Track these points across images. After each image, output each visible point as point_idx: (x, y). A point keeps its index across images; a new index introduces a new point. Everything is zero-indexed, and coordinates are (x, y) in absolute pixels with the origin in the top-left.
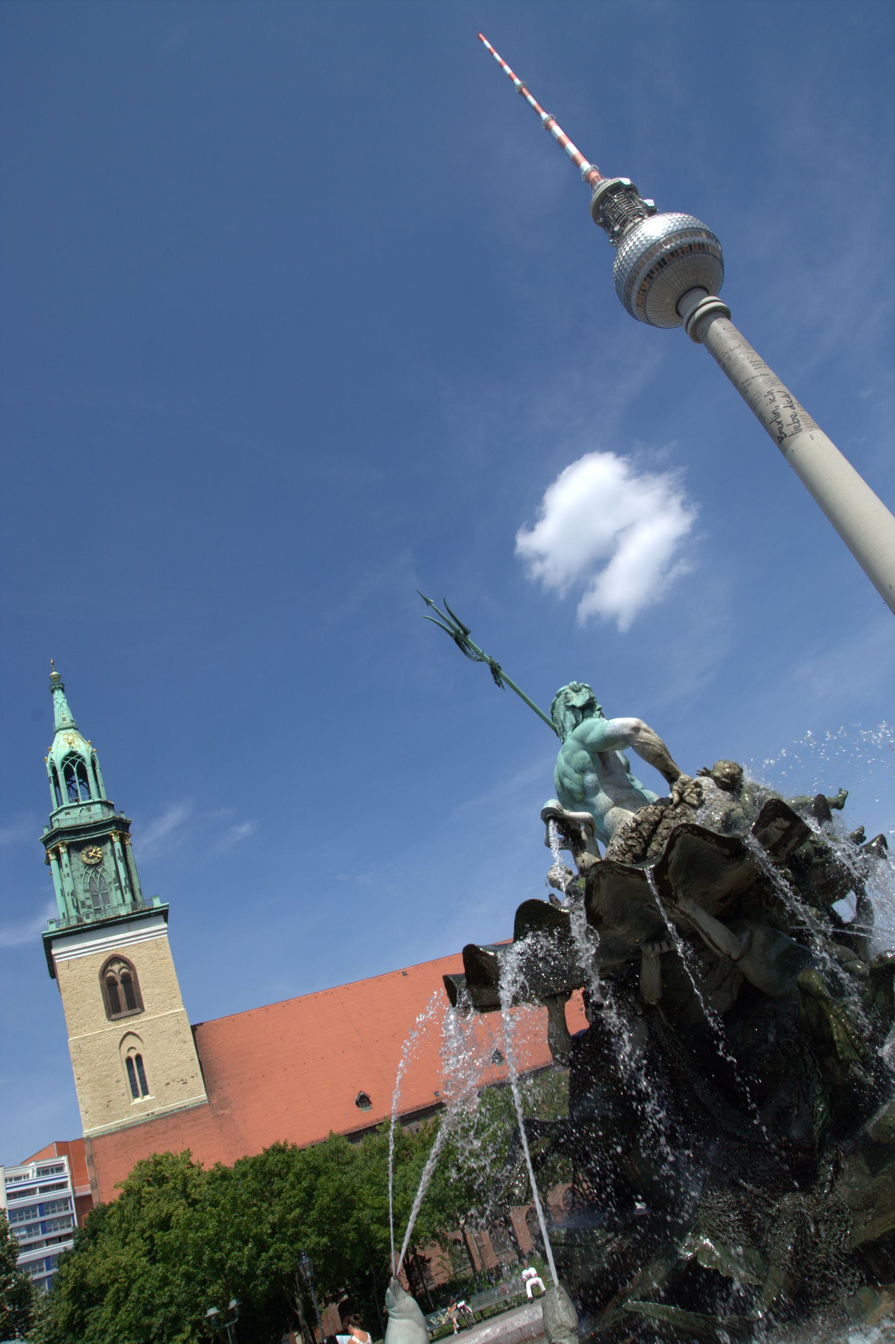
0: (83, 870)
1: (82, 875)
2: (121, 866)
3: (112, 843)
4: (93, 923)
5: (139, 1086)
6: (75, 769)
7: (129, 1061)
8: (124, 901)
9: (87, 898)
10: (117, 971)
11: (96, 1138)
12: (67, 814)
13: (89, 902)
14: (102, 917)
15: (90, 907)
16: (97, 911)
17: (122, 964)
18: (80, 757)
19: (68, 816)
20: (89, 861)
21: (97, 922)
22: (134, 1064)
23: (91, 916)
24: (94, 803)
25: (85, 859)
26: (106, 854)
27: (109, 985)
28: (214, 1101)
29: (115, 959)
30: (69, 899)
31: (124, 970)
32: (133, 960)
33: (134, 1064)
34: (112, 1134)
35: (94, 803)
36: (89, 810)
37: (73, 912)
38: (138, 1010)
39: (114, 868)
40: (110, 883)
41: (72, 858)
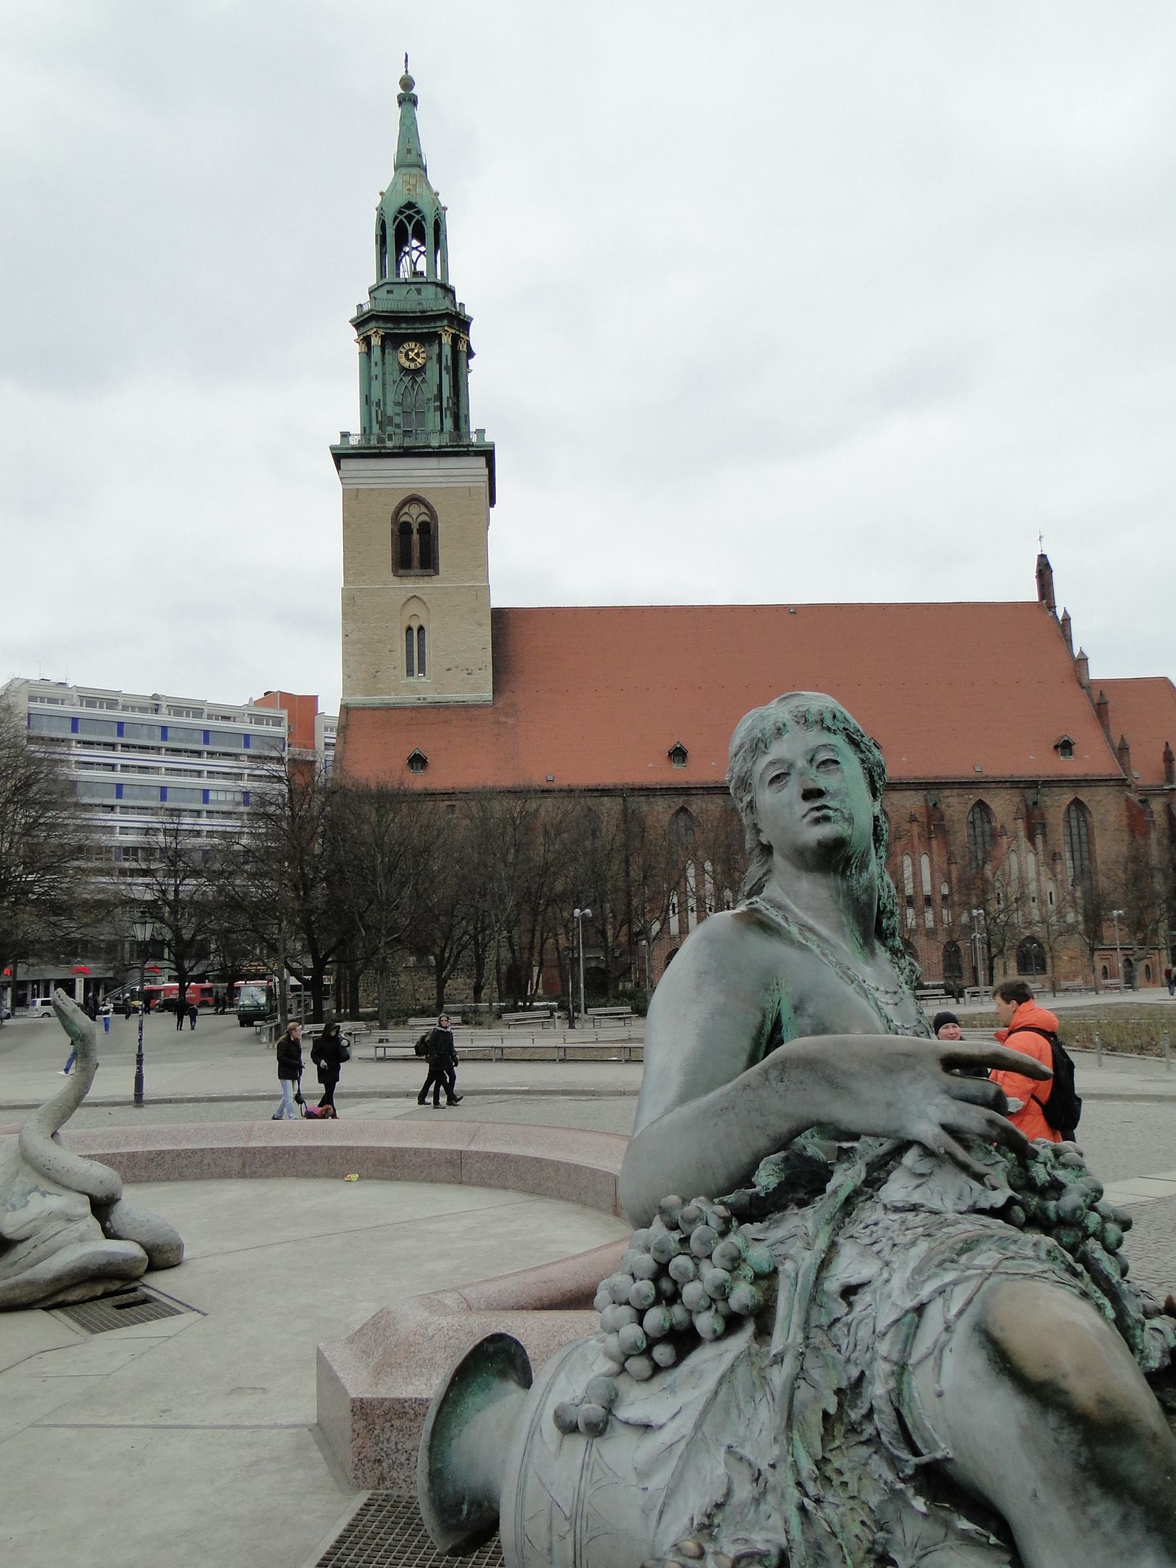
0: (397, 375)
1: (394, 382)
2: (446, 379)
4: (395, 447)
5: (416, 661)
6: (410, 229)
7: (409, 629)
8: (442, 429)
11: (356, 709)
12: (389, 292)
13: (397, 420)
14: (408, 442)
15: (398, 426)
16: (407, 433)
17: (424, 509)
18: (418, 212)
19: (390, 296)
20: (407, 364)
21: (400, 447)
22: (415, 636)
24: (427, 283)
25: (403, 360)
26: (431, 358)
27: (402, 531)
28: (498, 705)
29: (414, 500)
30: (374, 408)
31: (424, 518)
32: (437, 508)
33: (415, 636)
34: (374, 709)
35: (427, 283)
36: (419, 292)
37: (376, 428)
38: (431, 571)
41: (386, 356)
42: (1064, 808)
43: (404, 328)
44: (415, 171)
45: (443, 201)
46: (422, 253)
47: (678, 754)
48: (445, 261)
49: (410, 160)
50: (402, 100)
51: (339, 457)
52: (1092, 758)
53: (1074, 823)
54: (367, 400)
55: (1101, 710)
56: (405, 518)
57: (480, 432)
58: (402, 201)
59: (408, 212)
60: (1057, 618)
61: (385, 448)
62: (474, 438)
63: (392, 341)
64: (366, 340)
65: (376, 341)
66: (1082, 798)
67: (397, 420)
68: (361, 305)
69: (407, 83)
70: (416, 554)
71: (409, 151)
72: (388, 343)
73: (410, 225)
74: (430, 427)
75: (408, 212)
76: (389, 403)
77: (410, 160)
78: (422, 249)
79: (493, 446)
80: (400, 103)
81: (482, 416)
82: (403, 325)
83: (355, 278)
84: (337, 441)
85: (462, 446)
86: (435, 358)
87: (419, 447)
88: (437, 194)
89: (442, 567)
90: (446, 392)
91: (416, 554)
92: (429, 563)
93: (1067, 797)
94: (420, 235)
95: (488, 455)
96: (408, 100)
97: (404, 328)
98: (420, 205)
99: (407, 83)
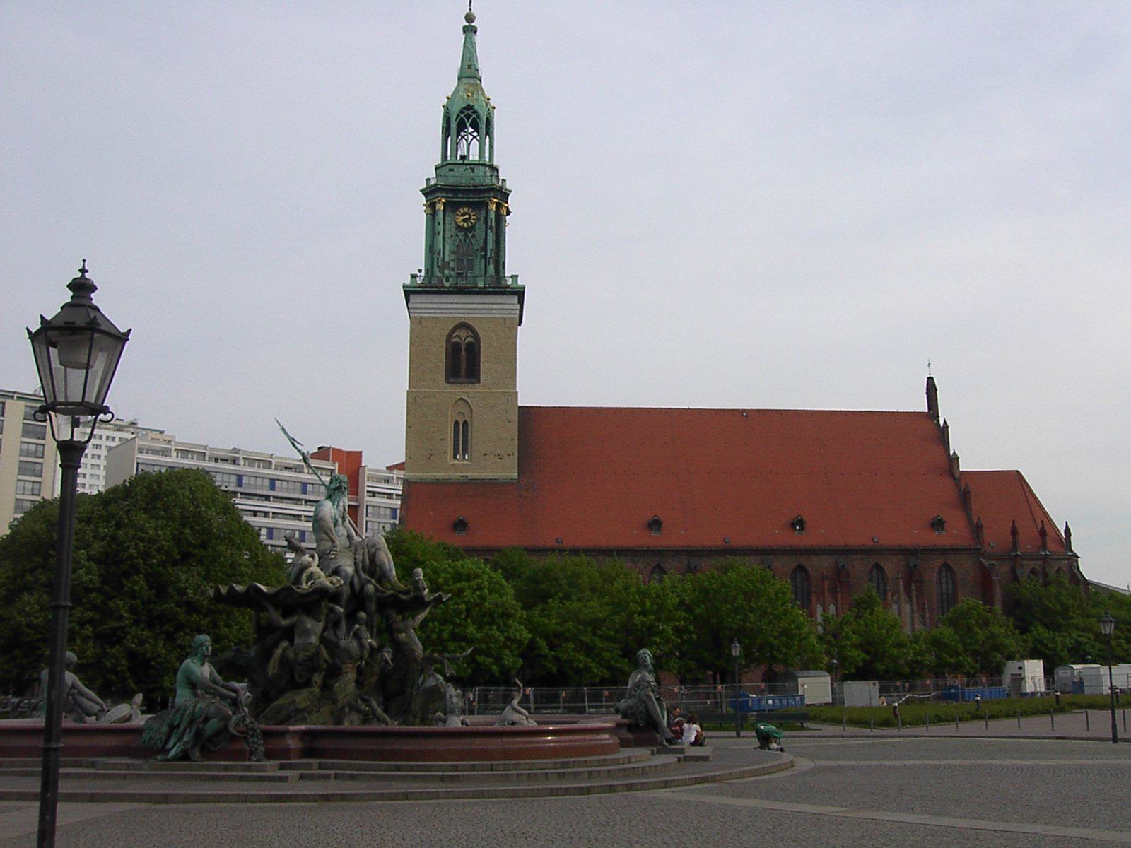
1: (452, 236)
2: (491, 237)
3: (487, 211)
4: (450, 287)
7: (457, 423)
9: (452, 261)
10: (463, 339)
12: (451, 170)
17: (470, 333)
18: (475, 112)
19: (451, 173)
21: (454, 288)
23: (450, 279)
27: (453, 350)
29: (464, 326)
36: (473, 170)
39: (484, 237)
40: (477, 250)
42: (936, 570)
43: (460, 198)
44: (472, 81)
45: (492, 103)
46: (475, 137)
47: (655, 524)
48: (491, 147)
49: (469, 73)
50: (465, 30)
51: (408, 293)
52: (956, 533)
53: (944, 581)
54: (431, 249)
55: (964, 499)
56: (457, 339)
57: (515, 277)
58: (464, 106)
59: (467, 112)
60: (939, 425)
61: (444, 287)
62: (509, 282)
63: (452, 206)
64: (431, 206)
65: (440, 207)
66: (950, 563)
67: (452, 265)
68: (429, 179)
69: (470, 18)
70: (463, 367)
71: (469, 67)
72: (448, 209)
73: (467, 118)
74: (477, 272)
75: (467, 112)
76: (447, 252)
77: (469, 73)
78: (475, 134)
79: (524, 288)
80: (464, 32)
81: (515, 264)
82: (460, 196)
83: (423, 157)
84: (408, 282)
85: (501, 288)
86: (482, 219)
87: (468, 288)
88: (489, 99)
89: (482, 377)
90: (490, 246)
91: (463, 367)
92: (472, 374)
93: (938, 562)
94: (475, 126)
95: (520, 294)
96: (470, 30)
97: (460, 198)
98: (476, 107)
99: (470, 18)
